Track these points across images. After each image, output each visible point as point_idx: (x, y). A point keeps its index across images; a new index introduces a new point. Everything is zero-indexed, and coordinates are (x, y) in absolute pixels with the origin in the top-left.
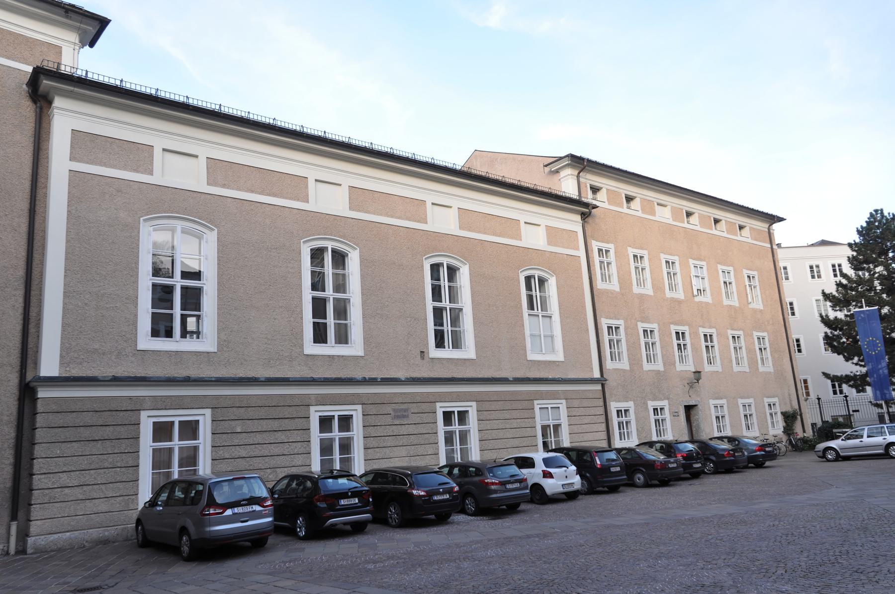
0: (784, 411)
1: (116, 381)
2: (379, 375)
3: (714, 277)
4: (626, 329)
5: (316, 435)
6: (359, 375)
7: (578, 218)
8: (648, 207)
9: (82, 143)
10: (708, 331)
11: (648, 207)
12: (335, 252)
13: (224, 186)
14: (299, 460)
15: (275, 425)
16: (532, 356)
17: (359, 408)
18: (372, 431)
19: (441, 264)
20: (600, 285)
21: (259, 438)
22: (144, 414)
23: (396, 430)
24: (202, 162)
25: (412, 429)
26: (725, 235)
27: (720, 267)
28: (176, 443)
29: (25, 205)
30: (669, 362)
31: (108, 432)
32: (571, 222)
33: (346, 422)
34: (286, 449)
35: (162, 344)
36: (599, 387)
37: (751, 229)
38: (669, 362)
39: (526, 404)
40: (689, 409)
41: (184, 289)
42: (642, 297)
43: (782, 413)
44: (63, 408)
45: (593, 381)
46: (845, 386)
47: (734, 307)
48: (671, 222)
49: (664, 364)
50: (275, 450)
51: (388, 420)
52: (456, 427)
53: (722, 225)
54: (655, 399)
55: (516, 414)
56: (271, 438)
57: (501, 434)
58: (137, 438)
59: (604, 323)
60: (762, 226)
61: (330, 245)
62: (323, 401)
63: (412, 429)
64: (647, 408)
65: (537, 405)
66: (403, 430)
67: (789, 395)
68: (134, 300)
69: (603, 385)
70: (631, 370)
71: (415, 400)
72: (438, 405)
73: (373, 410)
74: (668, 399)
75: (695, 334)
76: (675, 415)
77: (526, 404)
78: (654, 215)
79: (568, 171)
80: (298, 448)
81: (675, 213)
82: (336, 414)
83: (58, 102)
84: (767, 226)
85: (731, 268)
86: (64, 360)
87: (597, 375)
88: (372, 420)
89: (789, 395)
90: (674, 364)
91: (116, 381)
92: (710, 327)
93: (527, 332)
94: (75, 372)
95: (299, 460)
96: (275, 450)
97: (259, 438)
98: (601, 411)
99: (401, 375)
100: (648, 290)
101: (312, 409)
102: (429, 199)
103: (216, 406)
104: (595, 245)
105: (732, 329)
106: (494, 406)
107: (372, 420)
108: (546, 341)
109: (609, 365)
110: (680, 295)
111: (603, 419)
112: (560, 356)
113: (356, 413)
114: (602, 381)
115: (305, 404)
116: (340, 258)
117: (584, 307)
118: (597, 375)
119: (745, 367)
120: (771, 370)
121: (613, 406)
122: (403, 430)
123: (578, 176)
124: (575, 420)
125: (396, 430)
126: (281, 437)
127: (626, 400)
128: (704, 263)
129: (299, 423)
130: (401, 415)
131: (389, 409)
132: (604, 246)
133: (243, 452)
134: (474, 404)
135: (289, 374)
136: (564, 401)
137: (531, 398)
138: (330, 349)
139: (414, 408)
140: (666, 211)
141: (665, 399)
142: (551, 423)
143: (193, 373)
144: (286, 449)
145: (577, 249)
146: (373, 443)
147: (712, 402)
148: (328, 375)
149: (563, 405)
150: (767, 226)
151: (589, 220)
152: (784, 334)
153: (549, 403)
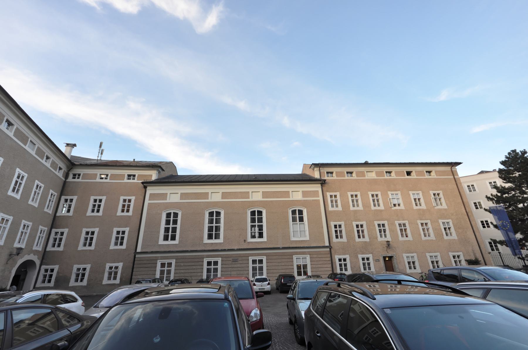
0: (468, 258)
1: (152, 252)
2: (227, 248)
3: (405, 197)
4: (345, 225)
5: (205, 267)
6: (220, 248)
7: (320, 185)
8: (358, 174)
9: (152, 196)
10: (402, 222)
11: (362, 174)
12: (216, 212)
13: (185, 199)
14: (199, 274)
15: (193, 264)
16: (293, 239)
17: (220, 259)
18: (224, 266)
19: (255, 211)
20: (330, 209)
21: (188, 267)
22: (158, 261)
23: (233, 266)
24: (179, 195)
25: (239, 265)
26: (415, 177)
27: (411, 193)
28: (166, 268)
29: (140, 212)
30: (373, 237)
31: (149, 265)
32: (317, 188)
33: (216, 263)
34: (195, 271)
35: (166, 243)
36: (328, 249)
37: (436, 172)
38: (373, 237)
39: (288, 257)
40: (391, 258)
41: (173, 228)
42: (355, 212)
43: (465, 260)
44: (141, 259)
45: (326, 247)
46: (499, 245)
47: (423, 210)
48: (376, 178)
49: (370, 238)
50: (192, 271)
51: (230, 262)
52: (258, 265)
53: (413, 174)
54: (363, 253)
55: (283, 260)
56: (191, 267)
57: (277, 268)
58: (156, 267)
59: (332, 224)
60: (448, 168)
61: (215, 210)
62: (208, 256)
63: (239, 265)
64: (357, 257)
65: (295, 257)
66: (236, 266)
67: (473, 251)
68: (159, 232)
69: (330, 249)
70: (348, 241)
71: (240, 256)
72: (250, 257)
73: (225, 259)
74: (372, 253)
75: (392, 224)
76: (377, 261)
77: (288, 257)
78: (365, 176)
79: (315, 169)
80: (199, 271)
81: (378, 174)
82: (257, 259)
83: (148, 188)
84: (450, 168)
85: (420, 192)
86: (142, 249)
87: (327, 244)
88: (224, 262)
89: (473, 251)
90: (377, 238)
91: (152, 252)
92: (404, 220)
93: (291, 230)
94: (144, 251)
95: (199, 274)
96: (192, 271)
97: (188, 267)
98: (329, 259)
99: (236, 248)
100: (361, 207)
101: (205, 259)
102: (250, 191)
103: (177, 258)
104: (328, 194)
105: (421, 220)
106: (275, 257)
107: (224, 262)
108: (300, 233)
109: (334, 240)
110: (382, 207)
111: (330, 262)
112: (307, 238)
113: (219, 260)
114: (330, 247)
115: (203, 257)
116: (218, 214)
117: (321, 218)
118: (327, 244)
119: (433, 237)
120: (456, 238)
121: (337, 257)
122: (236, 266)
123: (320, 170)
124: (313, 263)
125: (233, 266)
126: (194, 267)
127: (345, 254)
128: (399, 192)
129: (200, 263)
130: (235, 261)
131: (231, 259)
132: (333, 194)
133: (183, 271)
134: (265, 257)
135: (199, 249)
136: (309, 256)
137: (292, 254)
138: (214, 241)
139: (240, 259)
140: (372, 175)
141: (370, 253)
142: (302, 264)
143: (172, 249)
144: (195, 271)
145: (318, 197)
146: (224, 270)
147: (405, 255)
148: (210, 249)
149: (308, 257)
150: (450, 168)
151: (326, 185)
152: (468, 219)
153: (301, 256)
